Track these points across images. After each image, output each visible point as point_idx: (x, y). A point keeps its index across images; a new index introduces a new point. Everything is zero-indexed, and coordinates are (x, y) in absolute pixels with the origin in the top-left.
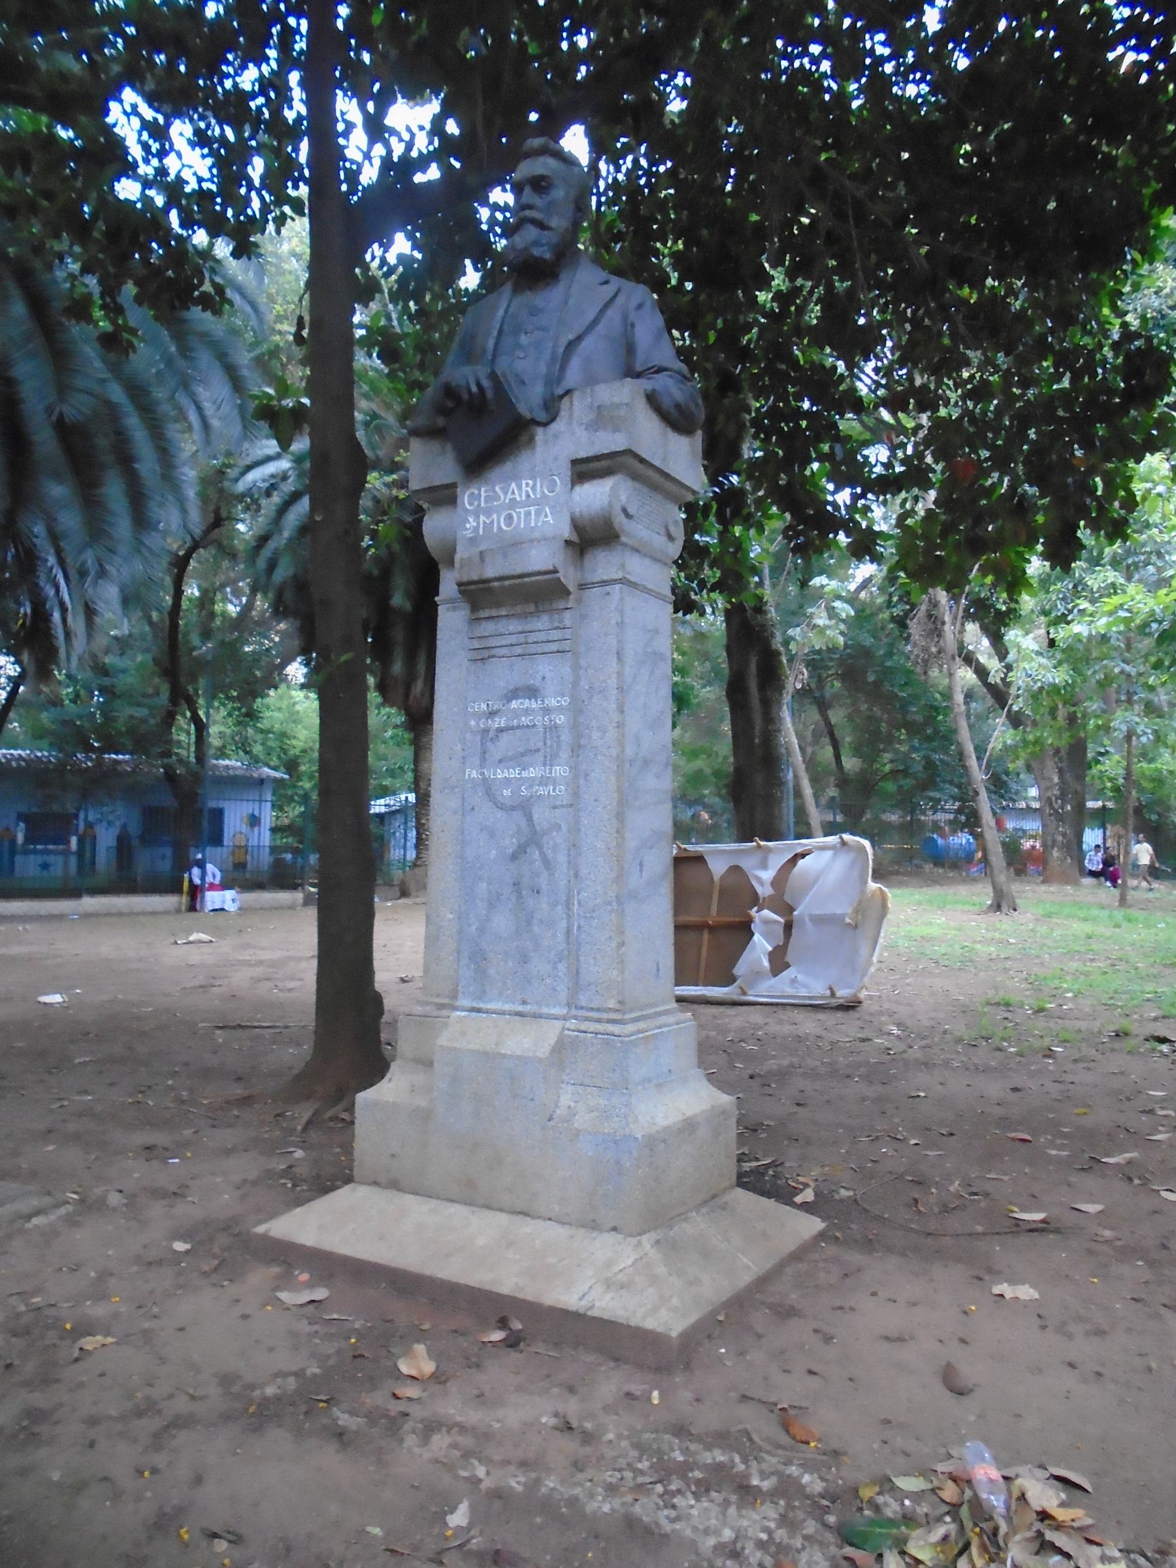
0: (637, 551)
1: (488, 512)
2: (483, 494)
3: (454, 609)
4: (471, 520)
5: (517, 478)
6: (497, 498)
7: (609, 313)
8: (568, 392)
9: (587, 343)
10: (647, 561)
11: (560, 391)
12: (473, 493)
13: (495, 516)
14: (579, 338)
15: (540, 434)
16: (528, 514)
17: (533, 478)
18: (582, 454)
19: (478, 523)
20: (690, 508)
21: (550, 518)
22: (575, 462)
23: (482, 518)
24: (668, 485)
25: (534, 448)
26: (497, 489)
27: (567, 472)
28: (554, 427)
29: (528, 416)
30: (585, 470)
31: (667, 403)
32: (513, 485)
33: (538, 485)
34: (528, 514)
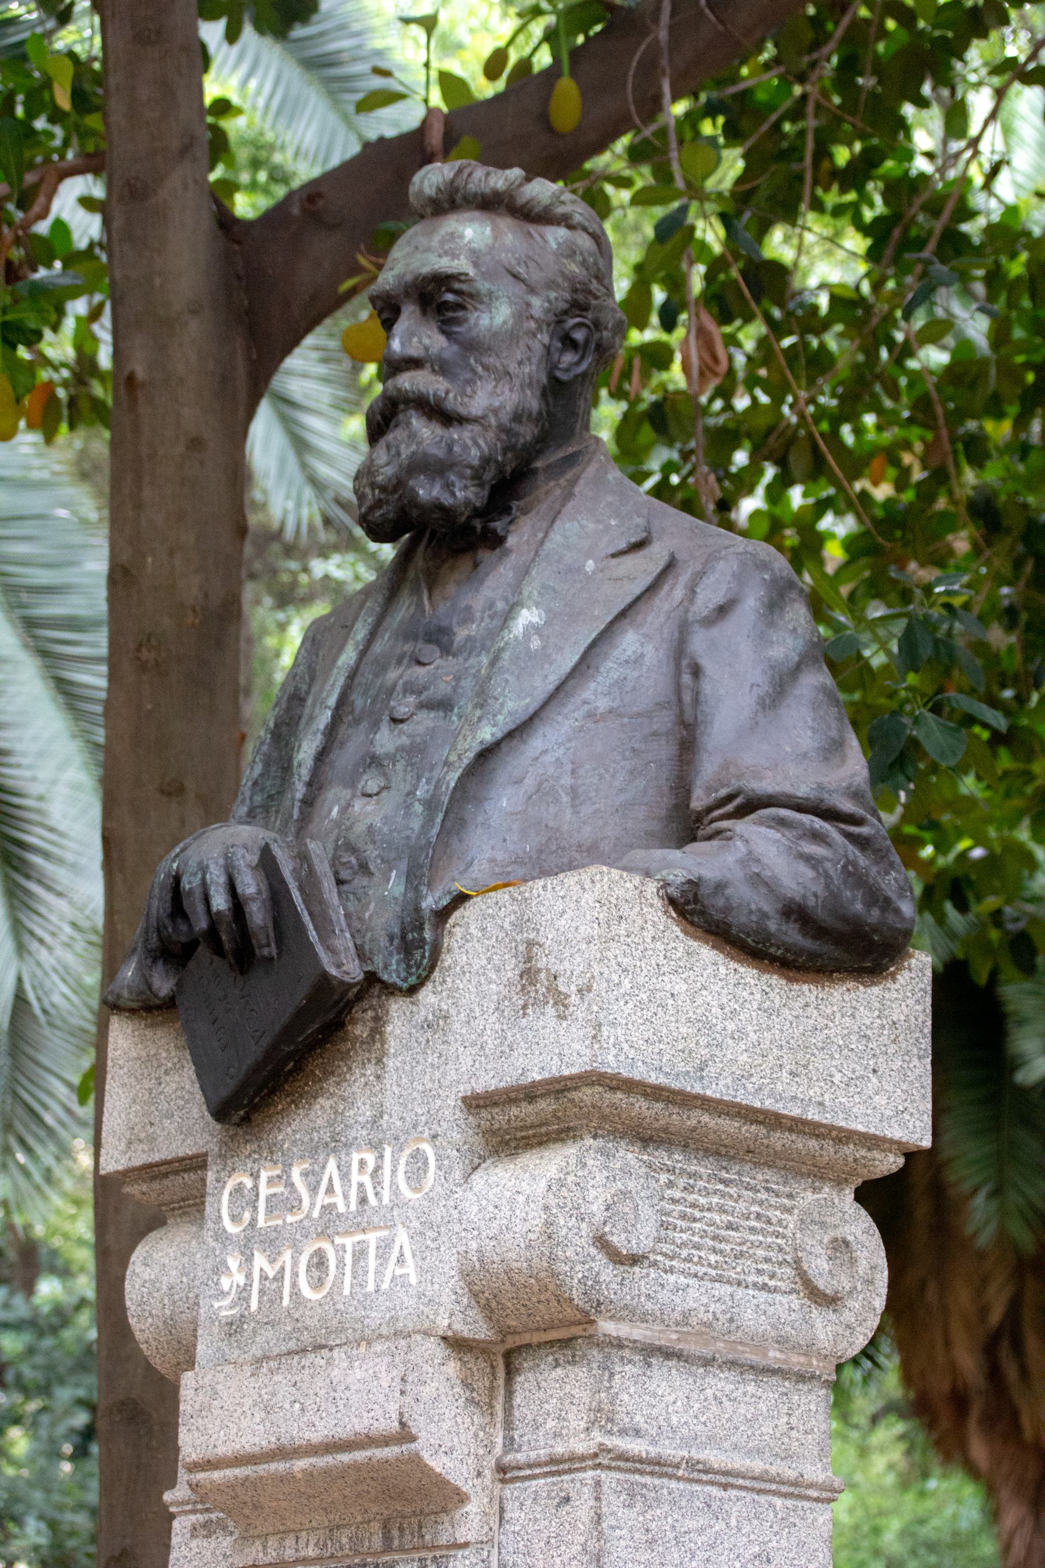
0: (668, 1354)
2: (264, 1191)
4: (233, 1263)
5: (338, 1144)
6: (292, 1204)
7: (629, 642)
8: (461, 899)
9: (548, 744)
10: (721, 1382)
11: (430, 902)
12: (239, 1189)
13: (287, 1256)
14: (520, 731)
15: (400, 1019)
16: (360, 1254)
17: (376, 1146)
18: (487, 1082)
19: (249, 1276)
20: (881, 1199)
23: (260, 1261)
24: (779, 1139)
25: (379, 1061)
26: (296, 1174)
27: (456, 1128)
28: (427, 996)
29: (352, 971)
30: (515, 1121)
31: (750, 903)
32: (332, 1165)
34: (360, 1254)
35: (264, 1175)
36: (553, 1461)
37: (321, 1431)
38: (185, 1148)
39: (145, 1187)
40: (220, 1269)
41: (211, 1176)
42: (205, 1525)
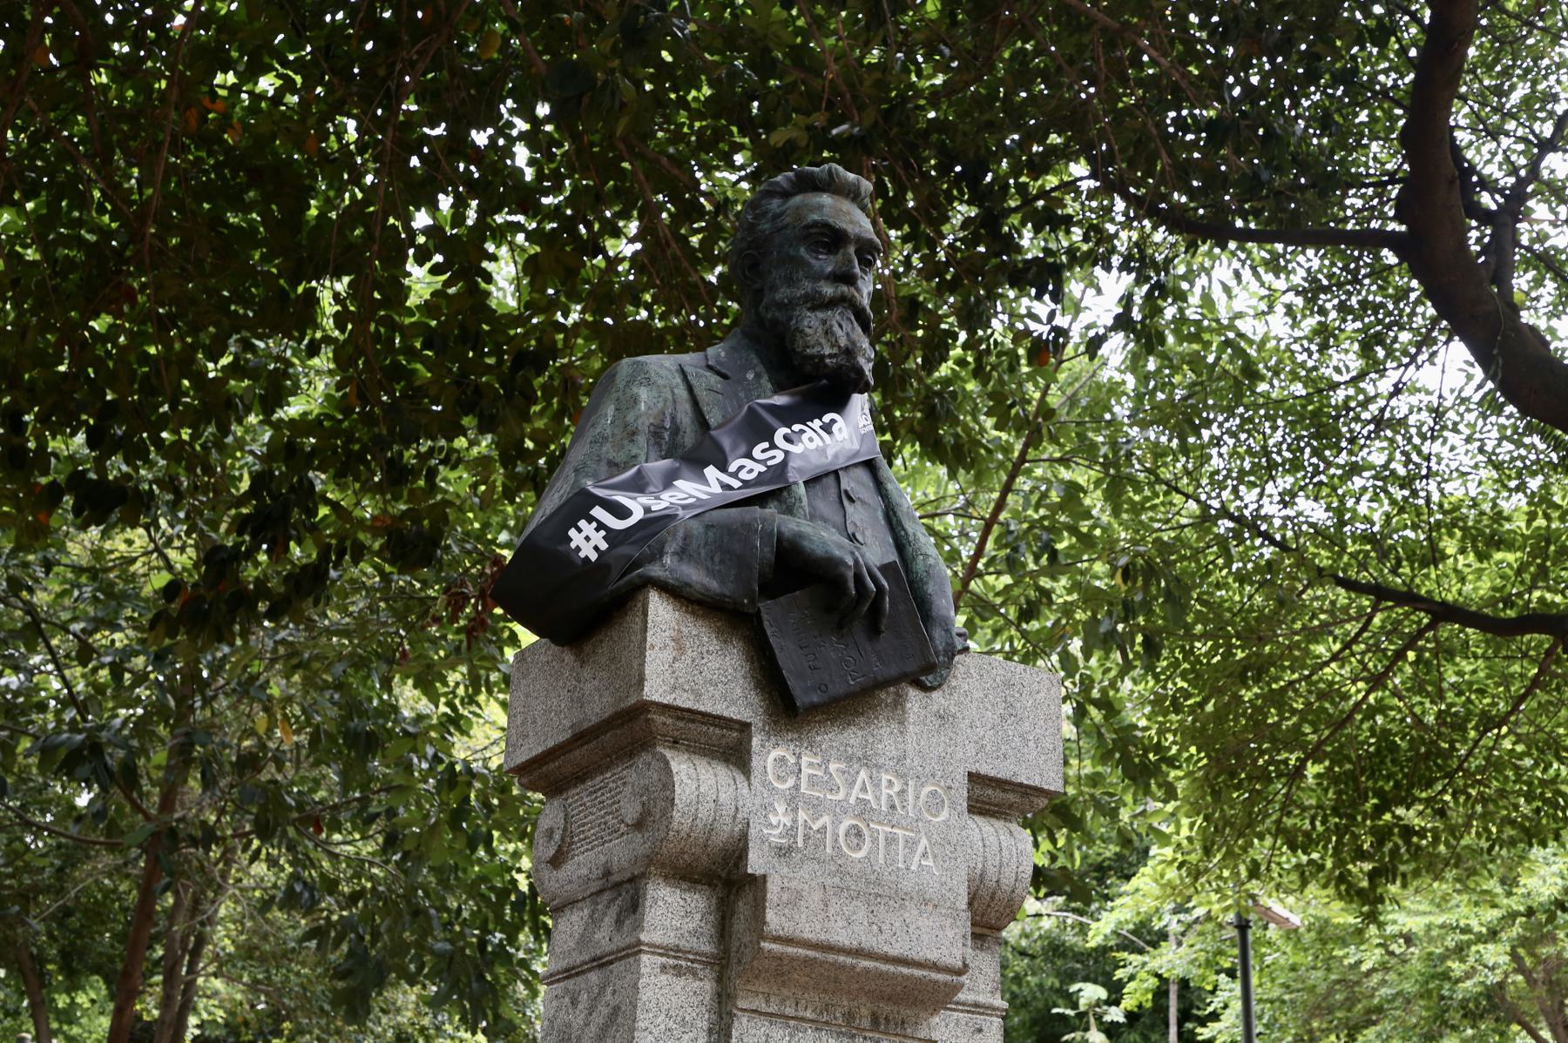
1: (816, 807)
3: (678, 971)
18: (985, 769)
19: (795, 821)
21: (929, 862)
22: (974, 778)
23: (802, 815)
25: (901, 723)
32: (863, 775)
33: (910, 790)
35: (805, 760)
36: (976, 1005)
37: (894, 951)
38: (732, 712)
39: (669, 721)
40: (767, 808)
41: (755, 741)
42: (675, 967)
